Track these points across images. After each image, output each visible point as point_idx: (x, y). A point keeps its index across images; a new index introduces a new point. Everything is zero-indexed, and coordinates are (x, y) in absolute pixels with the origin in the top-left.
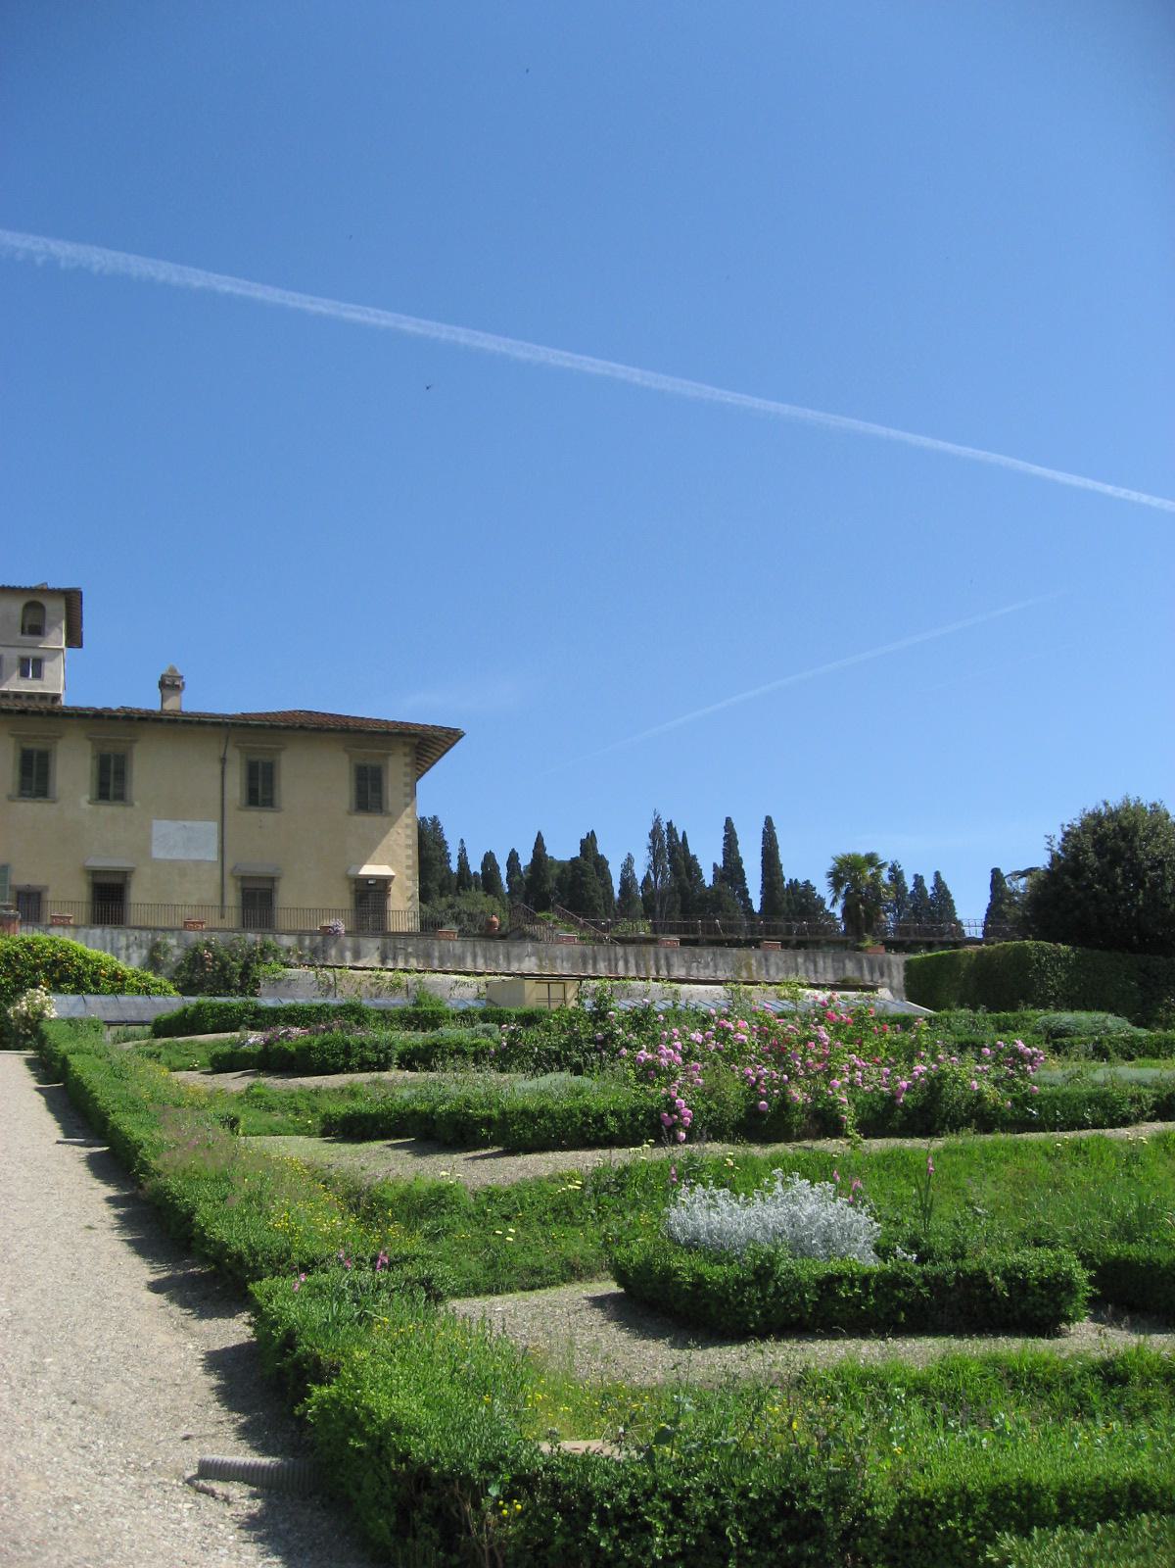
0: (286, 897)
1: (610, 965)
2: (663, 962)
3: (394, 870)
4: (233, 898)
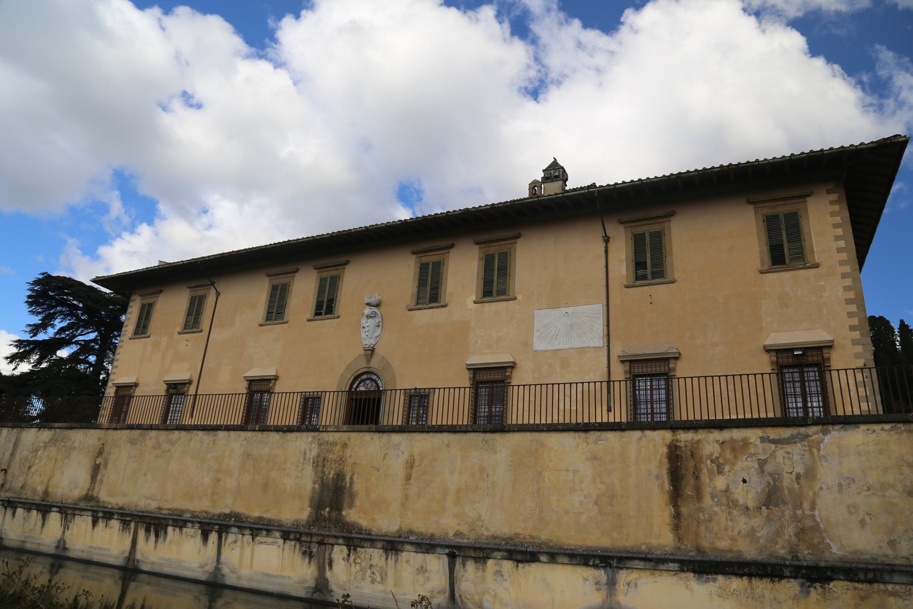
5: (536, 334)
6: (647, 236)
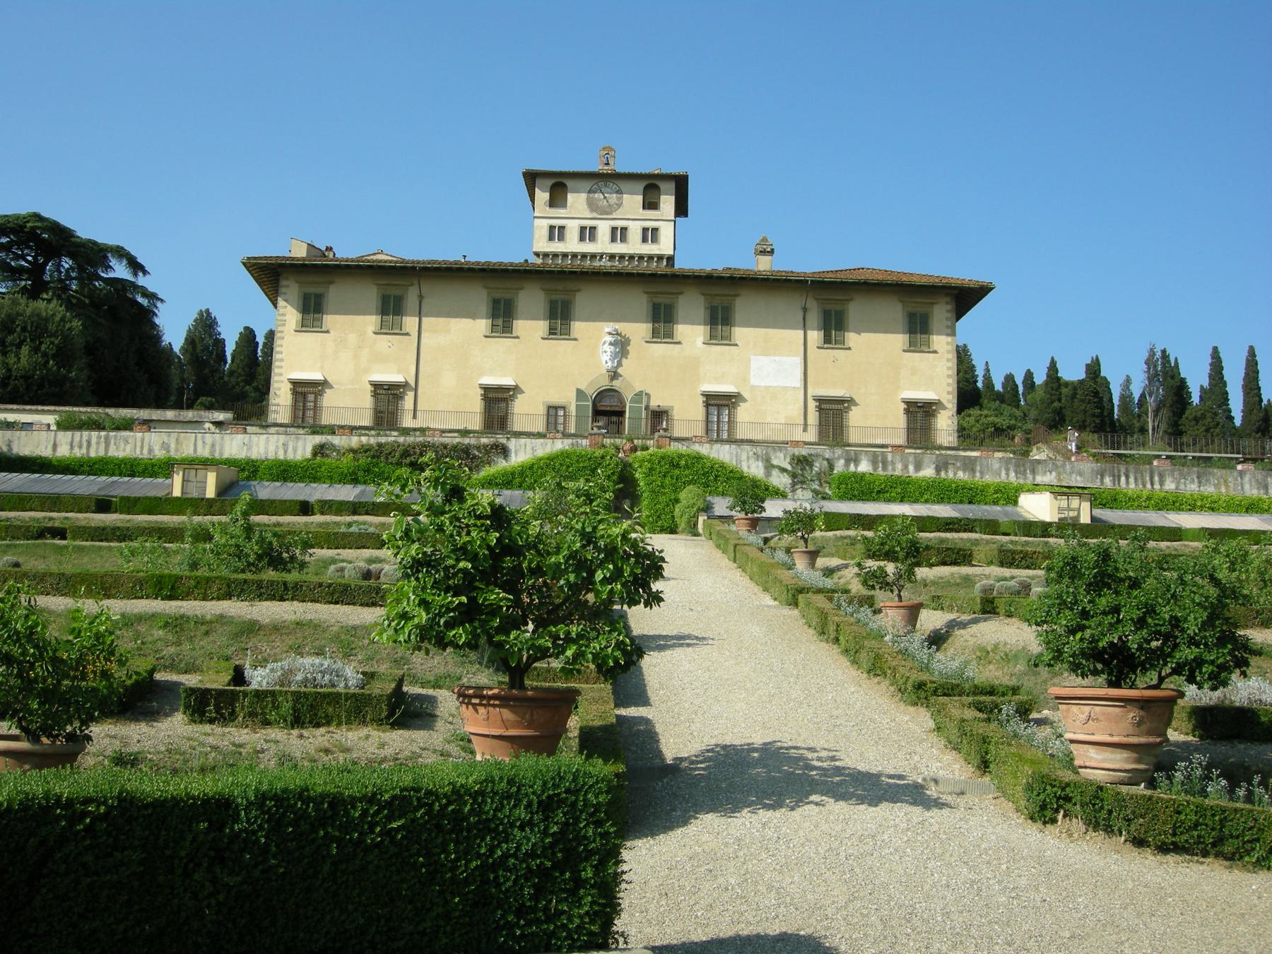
0: (855, 418)
1: (1114, 480)
2: (1156, 478)
3: (937, 395)
4: (813, 417)
5: (752, 373)
6: (833, 313)
